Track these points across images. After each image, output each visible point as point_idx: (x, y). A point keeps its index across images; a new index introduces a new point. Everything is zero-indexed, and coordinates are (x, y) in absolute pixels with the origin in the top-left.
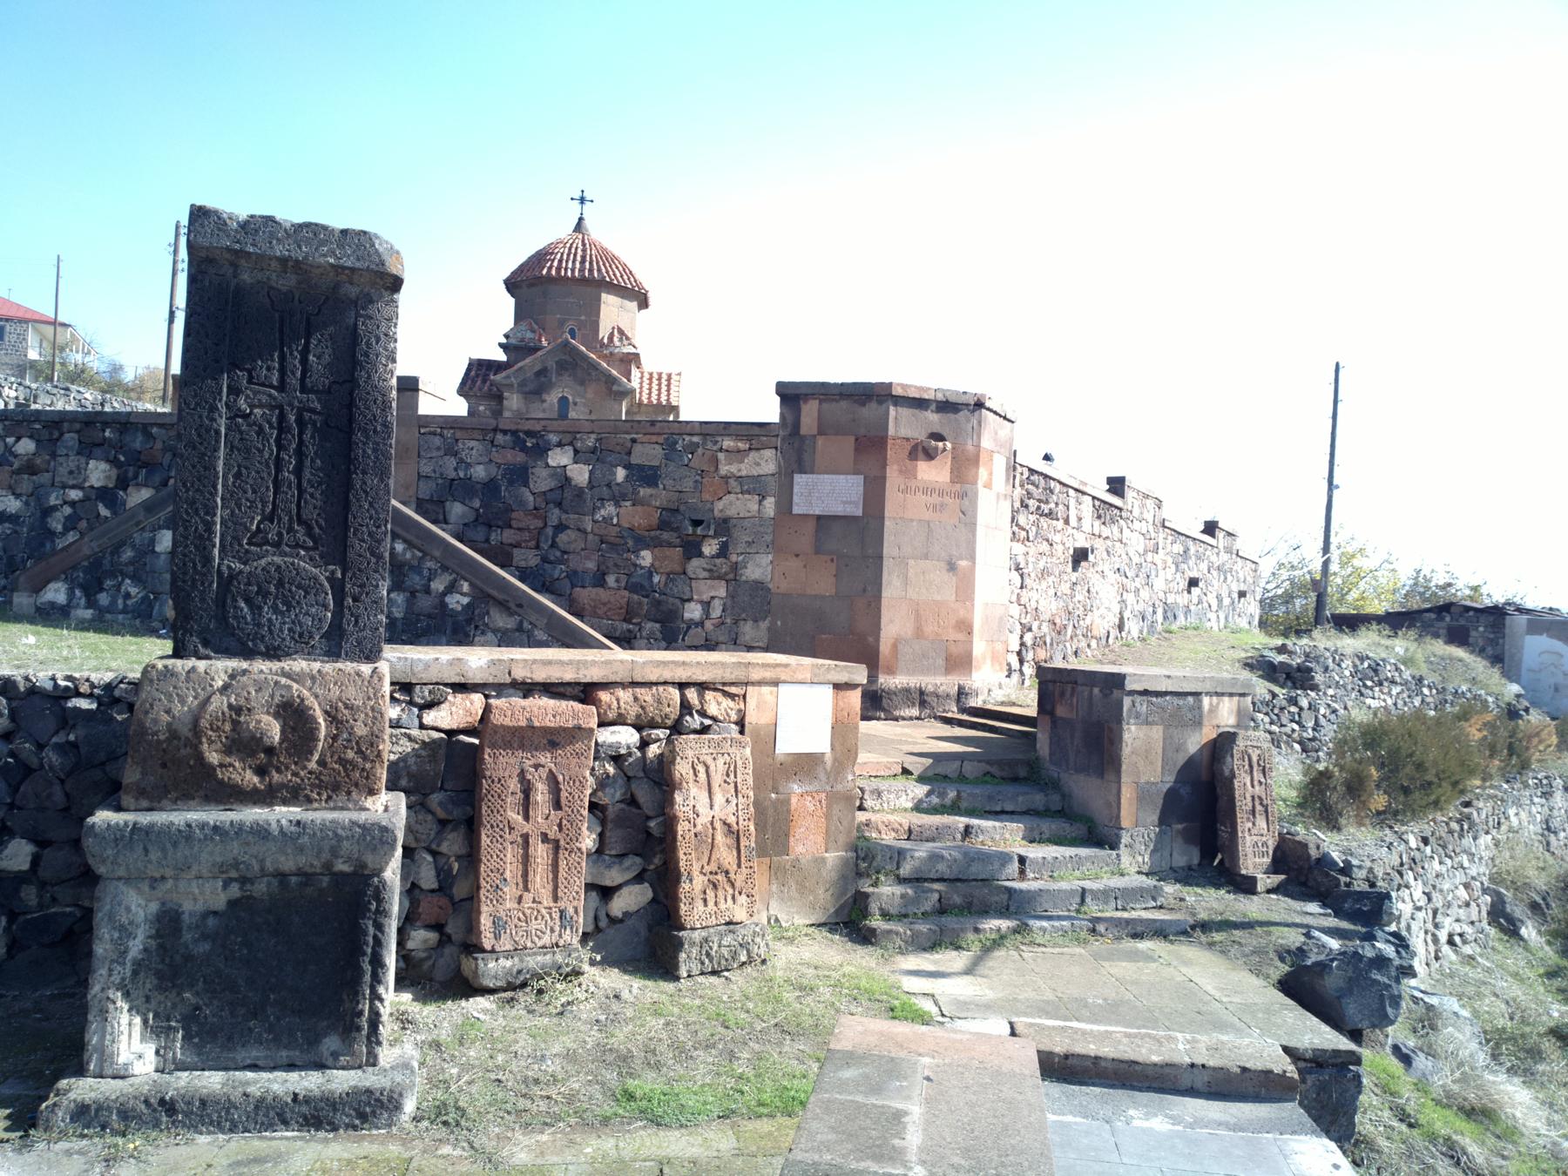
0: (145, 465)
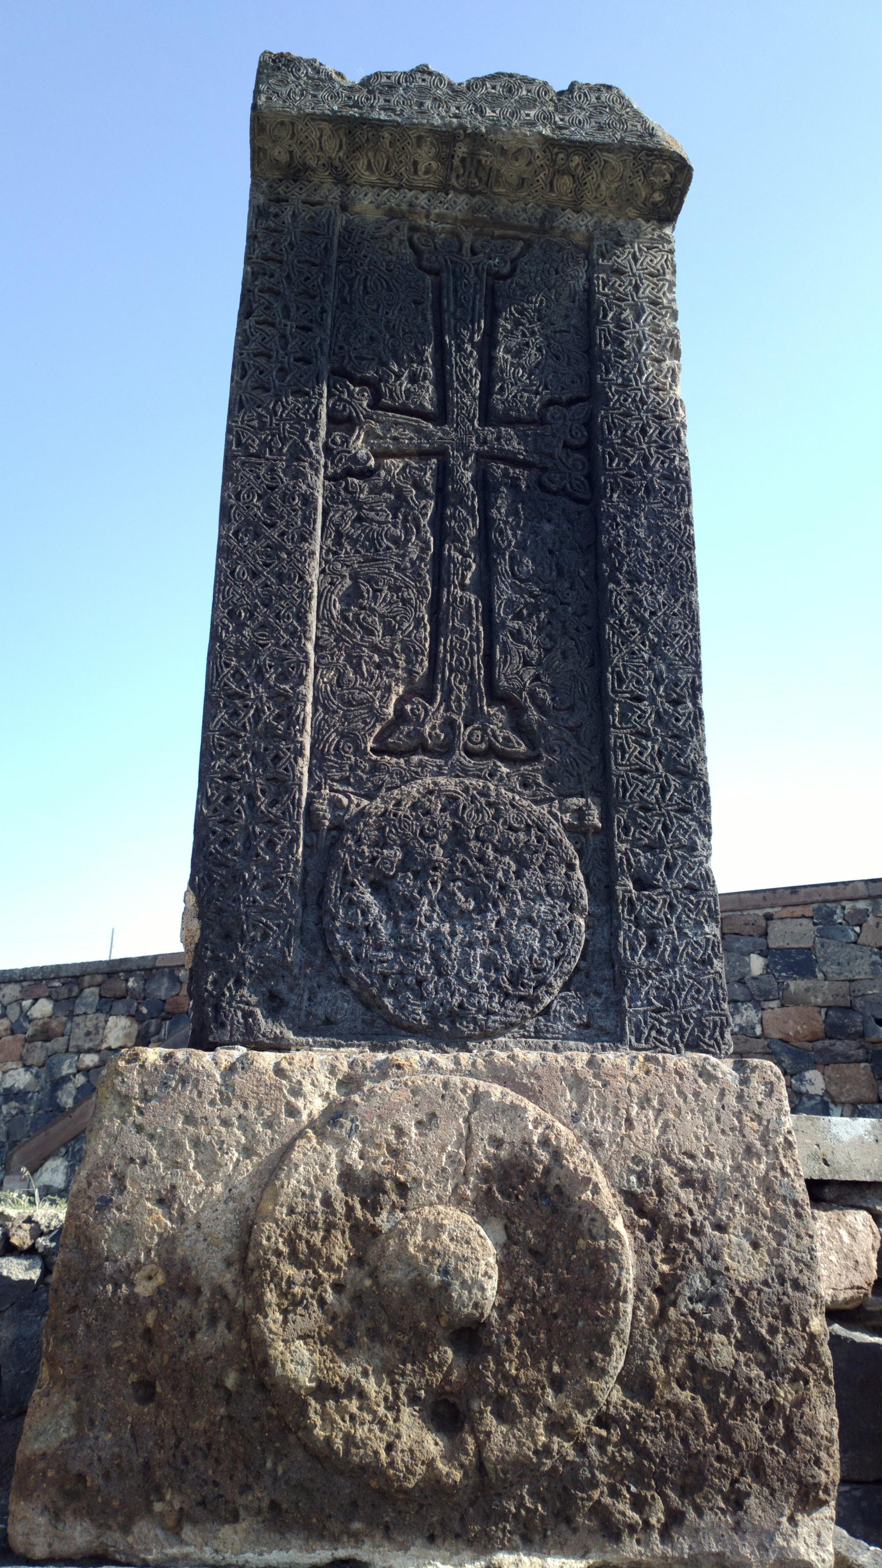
0: (170, 1016)
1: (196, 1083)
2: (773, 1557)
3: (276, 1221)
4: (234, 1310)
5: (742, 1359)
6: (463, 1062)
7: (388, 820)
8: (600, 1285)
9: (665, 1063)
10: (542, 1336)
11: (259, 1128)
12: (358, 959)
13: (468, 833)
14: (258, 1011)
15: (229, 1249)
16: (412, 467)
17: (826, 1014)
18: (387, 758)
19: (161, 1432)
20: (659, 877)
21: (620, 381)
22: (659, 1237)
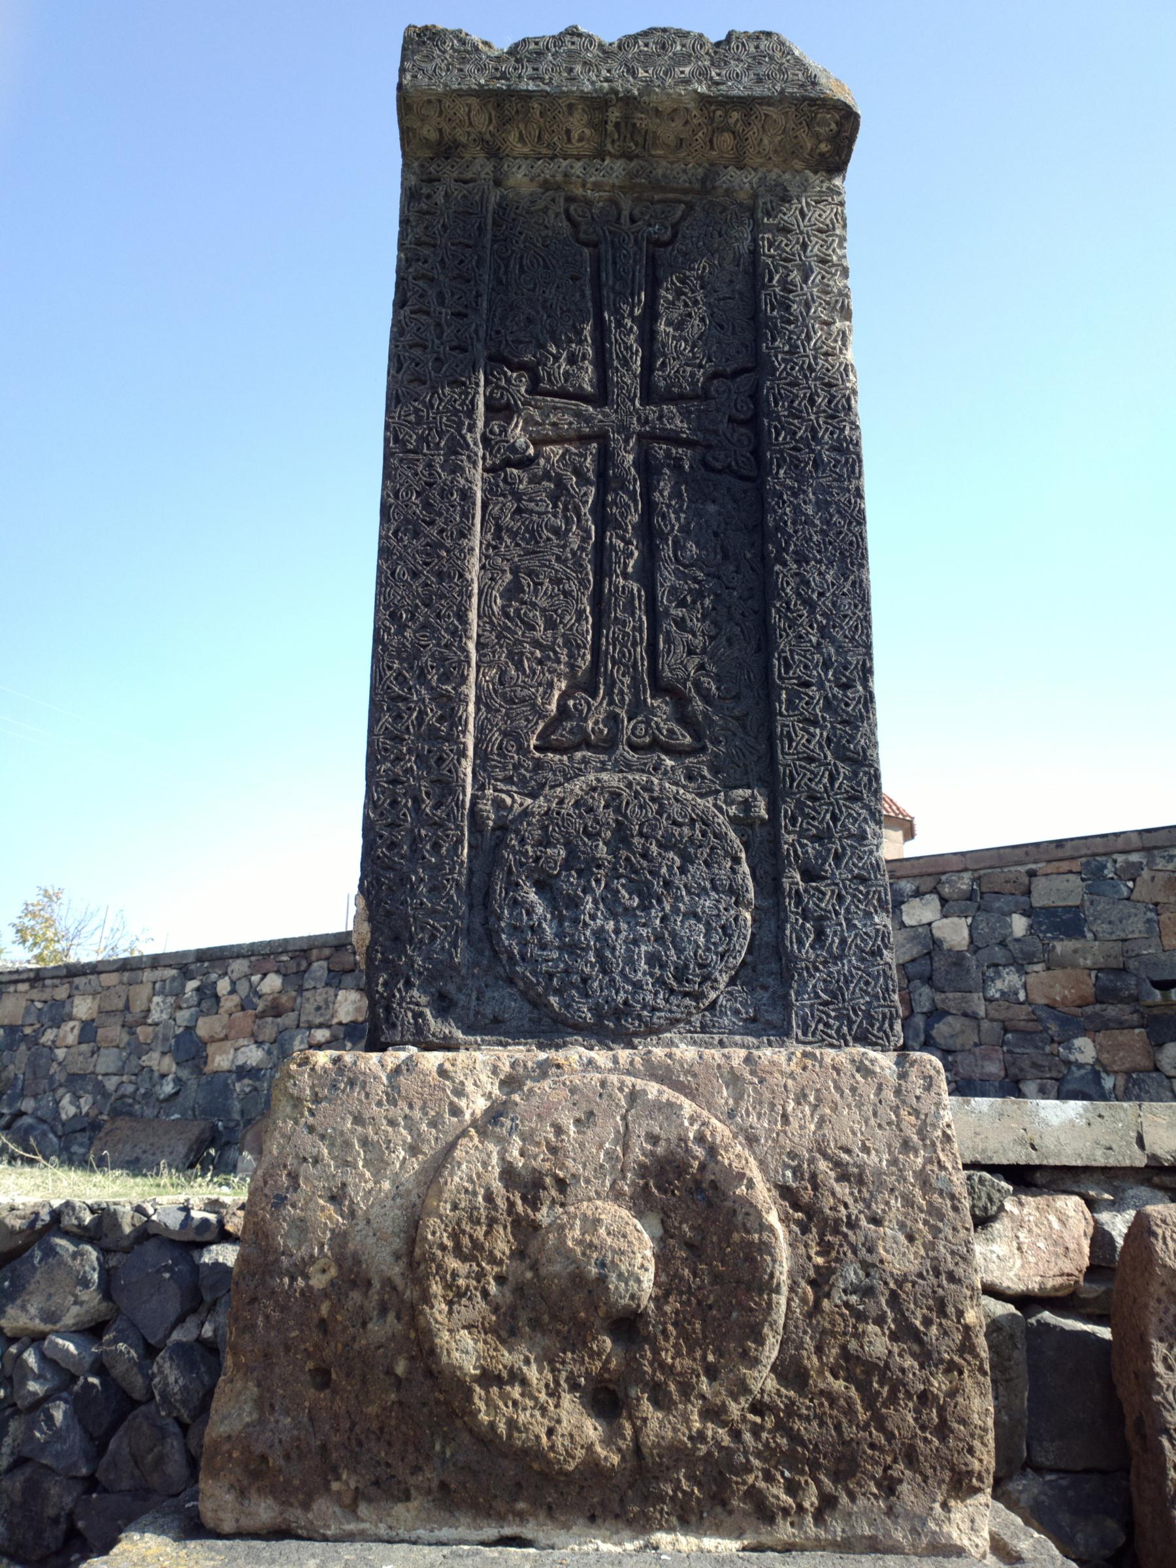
1: (364, 1085)
2: (925, 1540)
3: (440, 1217)
4: (403, 1301)
5: (896, 1350)
6: (621, 1061)
7: (551, 819)
8: (754, 1276)
9: (822, 1059)
10: (698, 1326)
11: (424, 1127)
12: (523, 959)
13: (631, 830)
14: (427, 1012)
15: (397, 1243)
16: (571, 454)
17: (1097, 977)
18: (550, 755)
19: (336, 1416)
20: (827, 867)
21: (787, 348)
22: (814, 1230)
